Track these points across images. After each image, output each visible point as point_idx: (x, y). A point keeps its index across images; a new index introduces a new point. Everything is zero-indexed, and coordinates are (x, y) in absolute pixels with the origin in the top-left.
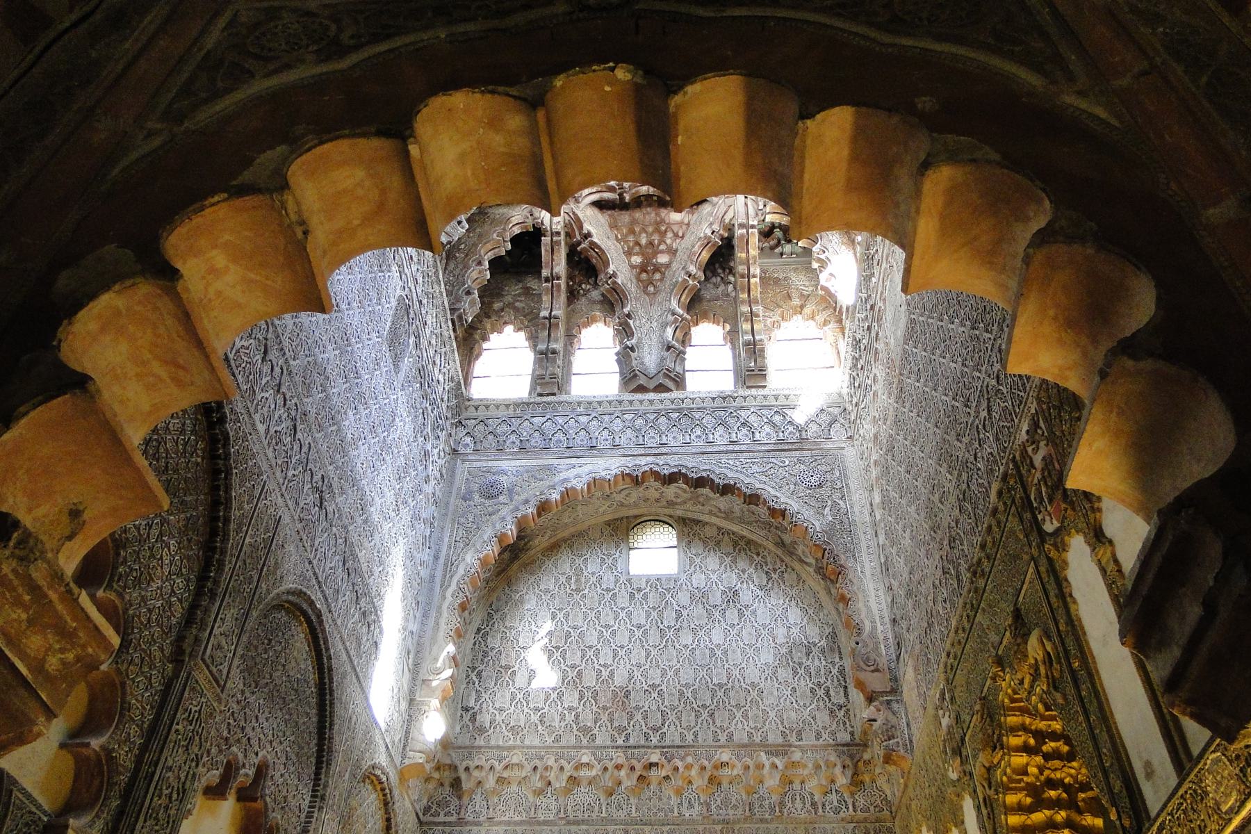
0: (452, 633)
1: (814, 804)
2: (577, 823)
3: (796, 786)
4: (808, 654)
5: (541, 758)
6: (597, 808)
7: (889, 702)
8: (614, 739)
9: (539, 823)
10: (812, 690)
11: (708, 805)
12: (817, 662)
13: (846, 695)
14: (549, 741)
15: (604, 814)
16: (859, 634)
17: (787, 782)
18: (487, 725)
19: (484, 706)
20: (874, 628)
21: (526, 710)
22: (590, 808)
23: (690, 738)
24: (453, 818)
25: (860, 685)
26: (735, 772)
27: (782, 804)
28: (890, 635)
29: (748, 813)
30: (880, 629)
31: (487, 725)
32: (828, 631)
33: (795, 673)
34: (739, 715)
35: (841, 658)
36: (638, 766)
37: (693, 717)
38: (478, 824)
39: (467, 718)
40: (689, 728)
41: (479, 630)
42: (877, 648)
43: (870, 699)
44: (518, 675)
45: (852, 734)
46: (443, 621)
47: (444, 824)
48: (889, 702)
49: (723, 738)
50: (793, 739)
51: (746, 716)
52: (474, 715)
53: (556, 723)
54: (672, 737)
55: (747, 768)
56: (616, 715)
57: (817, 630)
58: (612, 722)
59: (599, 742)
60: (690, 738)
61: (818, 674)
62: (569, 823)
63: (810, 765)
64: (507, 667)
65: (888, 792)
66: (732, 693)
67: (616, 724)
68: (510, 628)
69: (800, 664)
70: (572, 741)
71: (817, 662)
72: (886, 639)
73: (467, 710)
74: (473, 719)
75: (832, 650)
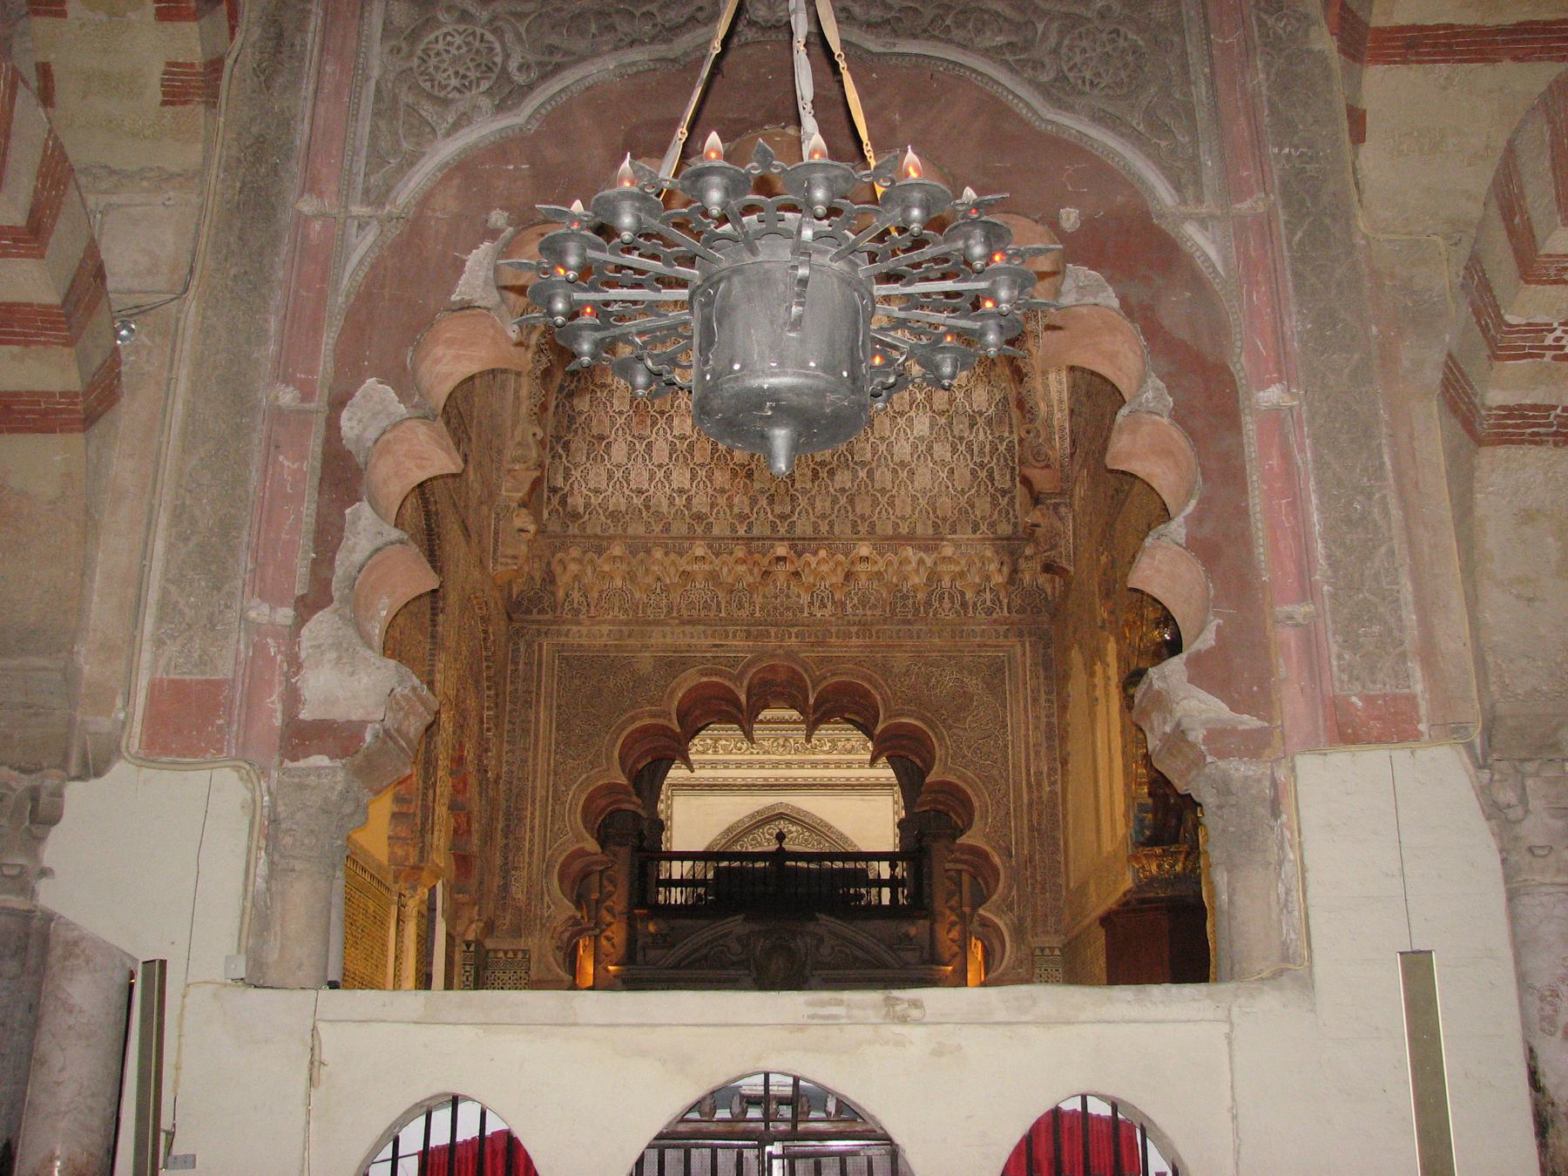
0: (536, 410)
1: (964, 605)
2: (691, 622)
3: (946, 583)
4: (972, 426)
5: (648, 552)
6: (714, 606)
7: (1056, 506)
8: (734, 529)
9: (649, 623)
10: (973, 473)
11: (843, 605)
12: (981, 437)
13: (1013, 479)
14: (657, 529)
15: (723, 614)
16: (1031, 421)
17: (933, 577)
18: (581, 510)
19: (576, 486)
20: (1050, 414)
21: (627, 492)
22: (707, 607)
23: (824, 528)
24: (549, 616)
25: (1026, 482)
26: (876, 569)
27: (928, 604)
28: (1067, 425)
29: (888, 614)
30: (1057, 415)
31: (581, 510)
32: (998, 397)
33: (954, 450)
34: (883, 500)
35: (1011, 432)
36: (765, 561)
37: (828, 504)
38: (579, 623)
39: (555, 501)
40: (824, 516)
41: (561, 388)
42: (1050, 440)
43: (1036, 499)
44: (615, 447)
45: (1015, 525)
46: (524, 392)
47: (539, 622)
48: (1056, 506)
49: (863, 528)
50: (945, 530)
51: (891, 504)
52: (565, 496)
53: (664, 509)
54: (803, 527)
55: (889, 563)
56: (736, 500)
57: (985, 396)
58: (731, 507)
59: (716, 531)
60: (824, 528)
61: (981, 452)
62: (683, 623)
63: (963, 562)
64: (601, 438)
65: (1049, 591)
66: (877, 475)
67: (736, 510)
68: (604, 386)
69: (961, 438)
70: (684, 531)
71: (982, 436)
72: (1062, 429)
73: (554, 490)
74: (563, 502)
75: (1001, 422)
